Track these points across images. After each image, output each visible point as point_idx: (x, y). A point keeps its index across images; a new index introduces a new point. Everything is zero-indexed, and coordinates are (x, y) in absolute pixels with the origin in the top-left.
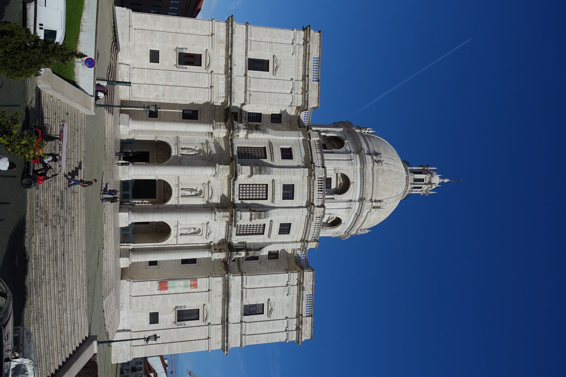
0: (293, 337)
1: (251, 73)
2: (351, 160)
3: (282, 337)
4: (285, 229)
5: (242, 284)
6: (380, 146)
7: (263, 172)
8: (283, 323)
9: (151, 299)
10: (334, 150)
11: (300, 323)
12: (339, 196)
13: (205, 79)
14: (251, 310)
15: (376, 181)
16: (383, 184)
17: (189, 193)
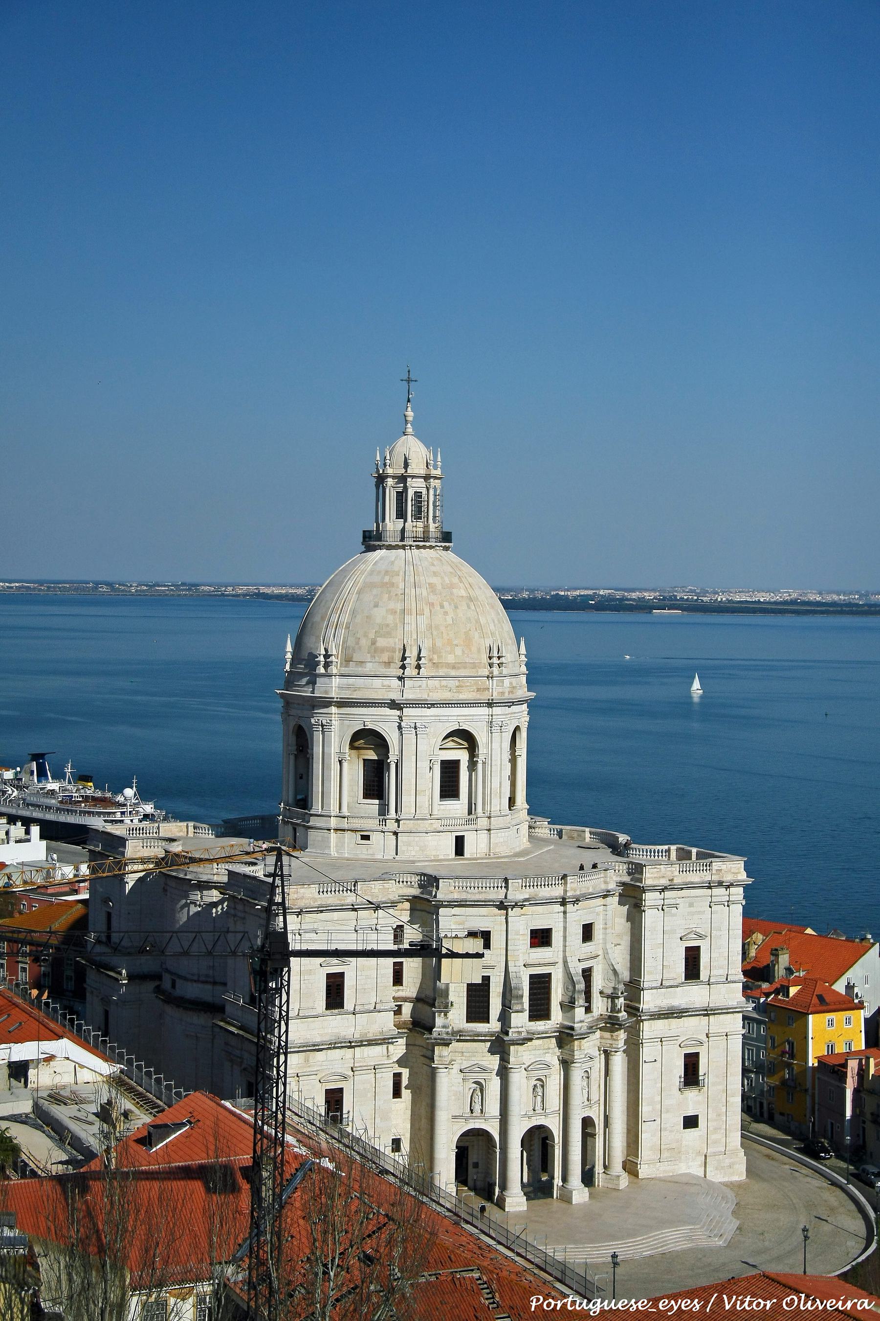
0: (738, 893)
1: (348, 1004)
2: (415, 728)
3: (737, 910)
4: (587, 933)
5: (656, 988)
6: (374, 643)
7: (520, 993)
8: (717, 912)
9: (666, 1129)
10: (392, 758)
11: (720, 884)
12: (482, 750)
13: (364, 1079)
14: (692, 969)
15: (454, 668)
16: (458, 651)
17: (539, 1099)
